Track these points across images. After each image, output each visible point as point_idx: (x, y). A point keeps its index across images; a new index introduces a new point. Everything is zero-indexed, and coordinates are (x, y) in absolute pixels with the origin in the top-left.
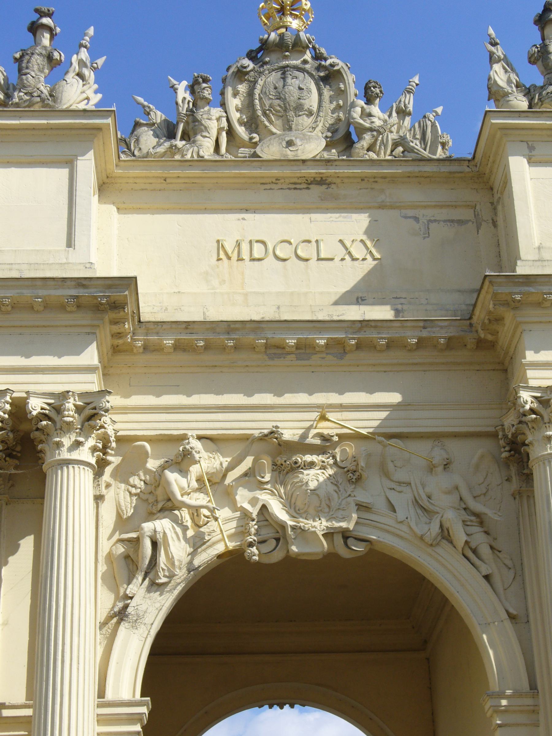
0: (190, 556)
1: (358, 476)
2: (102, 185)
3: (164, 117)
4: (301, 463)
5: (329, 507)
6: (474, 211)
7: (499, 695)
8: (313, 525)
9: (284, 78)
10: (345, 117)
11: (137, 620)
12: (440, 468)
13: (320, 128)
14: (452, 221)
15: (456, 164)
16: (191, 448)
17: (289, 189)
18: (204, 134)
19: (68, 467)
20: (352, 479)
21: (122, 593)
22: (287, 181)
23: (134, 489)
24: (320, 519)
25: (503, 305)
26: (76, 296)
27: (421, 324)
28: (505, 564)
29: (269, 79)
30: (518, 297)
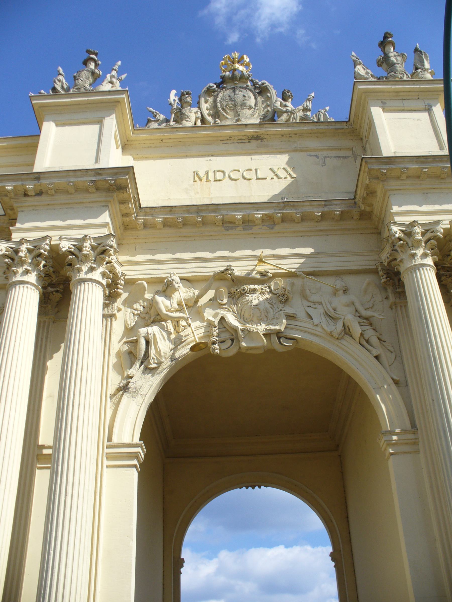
0: (172, 351)
1: (286, 297)
2: (124, 146)
3: (164, 117)
4: (247, 290)
5: (267, 317)
6: (352, 151)
7: (390, 433)
8: (256, 328)
9: (234, 92)
10: (271, 110)
11: (135, 391)
12: (341, 292)
13: (256, 115)
14: (339, 157)
15: (339, 124)
16: (172, 280)
17: (238, 143)
18: (187, 119)
19: (84, 284)
20: (282, 300)
21: (125, 375)
22: (237, 138)
23: (136, 311)
24: (261, 325)
25: (375, 178)
26: (95, 180)
27: (323, 203)
28: (388, 350)
29: (225, 93)
30: (385, 171)
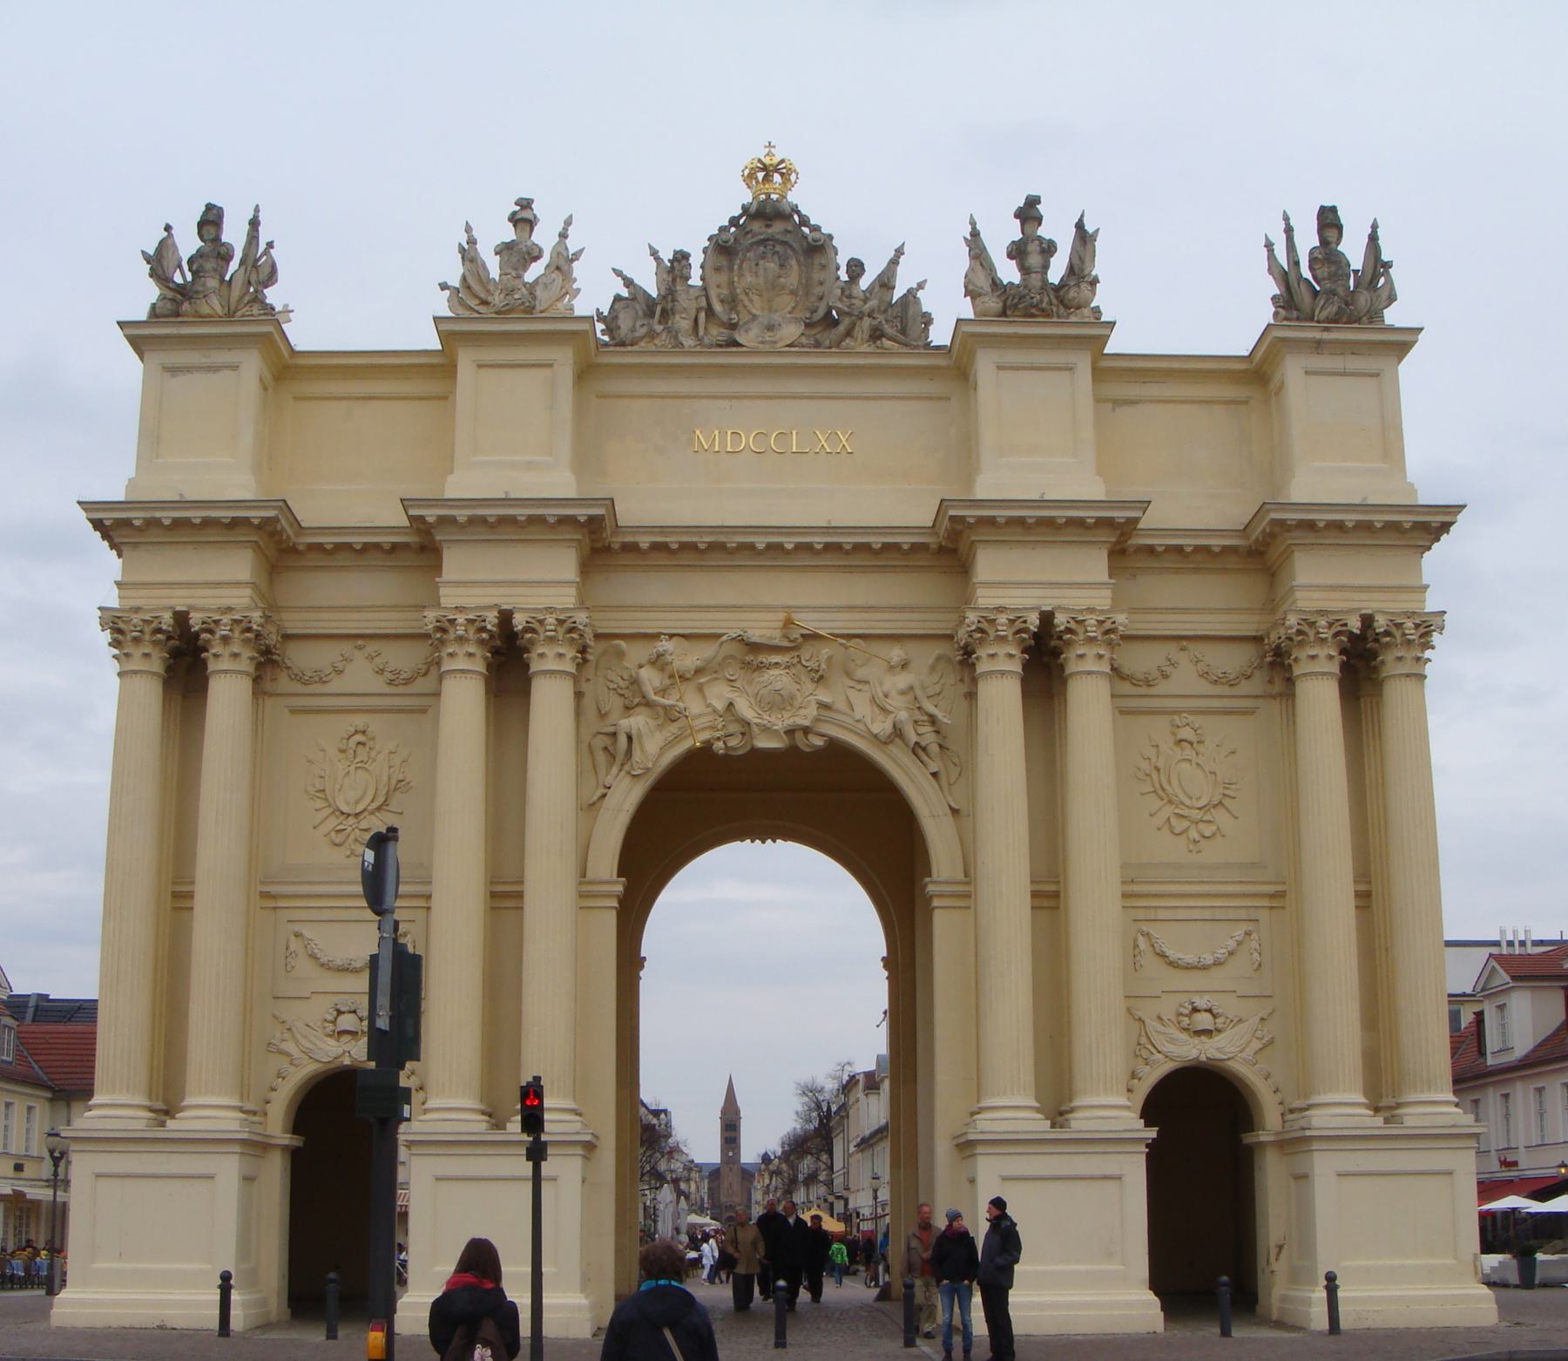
5: (791, 705)
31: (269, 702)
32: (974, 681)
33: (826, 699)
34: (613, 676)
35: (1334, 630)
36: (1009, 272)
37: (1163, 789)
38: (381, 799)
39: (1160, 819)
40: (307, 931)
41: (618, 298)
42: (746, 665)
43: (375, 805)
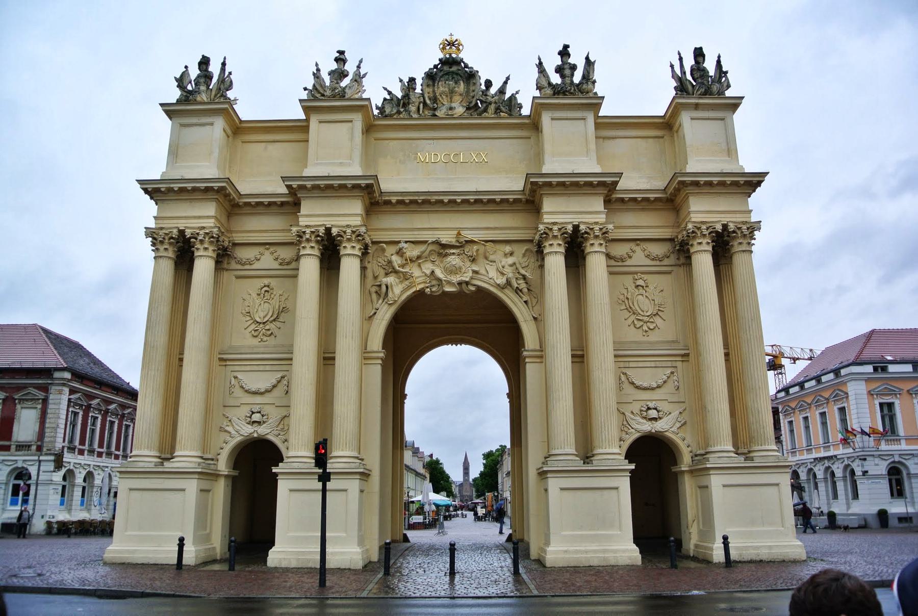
31: (226, 274)
32: (543, 259)
33: (476, 268)
34: (380, 260)
35: (709, 231)
36: (556, 79)
37: (630, 308)
38: (275, 316)
39: (630, 321)
40: (240, 375)
41: (385, 99)
42: (440, 254)
43: (272, 318)
